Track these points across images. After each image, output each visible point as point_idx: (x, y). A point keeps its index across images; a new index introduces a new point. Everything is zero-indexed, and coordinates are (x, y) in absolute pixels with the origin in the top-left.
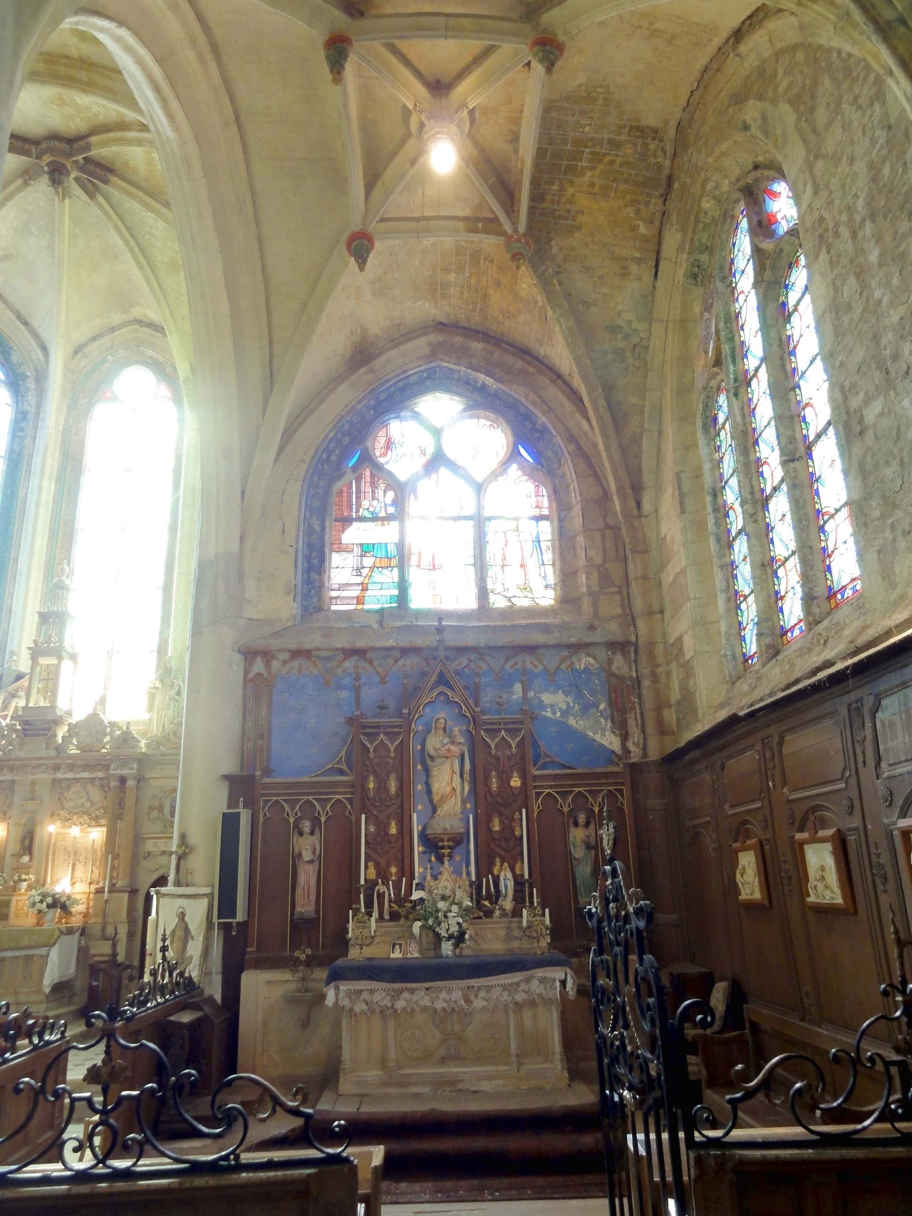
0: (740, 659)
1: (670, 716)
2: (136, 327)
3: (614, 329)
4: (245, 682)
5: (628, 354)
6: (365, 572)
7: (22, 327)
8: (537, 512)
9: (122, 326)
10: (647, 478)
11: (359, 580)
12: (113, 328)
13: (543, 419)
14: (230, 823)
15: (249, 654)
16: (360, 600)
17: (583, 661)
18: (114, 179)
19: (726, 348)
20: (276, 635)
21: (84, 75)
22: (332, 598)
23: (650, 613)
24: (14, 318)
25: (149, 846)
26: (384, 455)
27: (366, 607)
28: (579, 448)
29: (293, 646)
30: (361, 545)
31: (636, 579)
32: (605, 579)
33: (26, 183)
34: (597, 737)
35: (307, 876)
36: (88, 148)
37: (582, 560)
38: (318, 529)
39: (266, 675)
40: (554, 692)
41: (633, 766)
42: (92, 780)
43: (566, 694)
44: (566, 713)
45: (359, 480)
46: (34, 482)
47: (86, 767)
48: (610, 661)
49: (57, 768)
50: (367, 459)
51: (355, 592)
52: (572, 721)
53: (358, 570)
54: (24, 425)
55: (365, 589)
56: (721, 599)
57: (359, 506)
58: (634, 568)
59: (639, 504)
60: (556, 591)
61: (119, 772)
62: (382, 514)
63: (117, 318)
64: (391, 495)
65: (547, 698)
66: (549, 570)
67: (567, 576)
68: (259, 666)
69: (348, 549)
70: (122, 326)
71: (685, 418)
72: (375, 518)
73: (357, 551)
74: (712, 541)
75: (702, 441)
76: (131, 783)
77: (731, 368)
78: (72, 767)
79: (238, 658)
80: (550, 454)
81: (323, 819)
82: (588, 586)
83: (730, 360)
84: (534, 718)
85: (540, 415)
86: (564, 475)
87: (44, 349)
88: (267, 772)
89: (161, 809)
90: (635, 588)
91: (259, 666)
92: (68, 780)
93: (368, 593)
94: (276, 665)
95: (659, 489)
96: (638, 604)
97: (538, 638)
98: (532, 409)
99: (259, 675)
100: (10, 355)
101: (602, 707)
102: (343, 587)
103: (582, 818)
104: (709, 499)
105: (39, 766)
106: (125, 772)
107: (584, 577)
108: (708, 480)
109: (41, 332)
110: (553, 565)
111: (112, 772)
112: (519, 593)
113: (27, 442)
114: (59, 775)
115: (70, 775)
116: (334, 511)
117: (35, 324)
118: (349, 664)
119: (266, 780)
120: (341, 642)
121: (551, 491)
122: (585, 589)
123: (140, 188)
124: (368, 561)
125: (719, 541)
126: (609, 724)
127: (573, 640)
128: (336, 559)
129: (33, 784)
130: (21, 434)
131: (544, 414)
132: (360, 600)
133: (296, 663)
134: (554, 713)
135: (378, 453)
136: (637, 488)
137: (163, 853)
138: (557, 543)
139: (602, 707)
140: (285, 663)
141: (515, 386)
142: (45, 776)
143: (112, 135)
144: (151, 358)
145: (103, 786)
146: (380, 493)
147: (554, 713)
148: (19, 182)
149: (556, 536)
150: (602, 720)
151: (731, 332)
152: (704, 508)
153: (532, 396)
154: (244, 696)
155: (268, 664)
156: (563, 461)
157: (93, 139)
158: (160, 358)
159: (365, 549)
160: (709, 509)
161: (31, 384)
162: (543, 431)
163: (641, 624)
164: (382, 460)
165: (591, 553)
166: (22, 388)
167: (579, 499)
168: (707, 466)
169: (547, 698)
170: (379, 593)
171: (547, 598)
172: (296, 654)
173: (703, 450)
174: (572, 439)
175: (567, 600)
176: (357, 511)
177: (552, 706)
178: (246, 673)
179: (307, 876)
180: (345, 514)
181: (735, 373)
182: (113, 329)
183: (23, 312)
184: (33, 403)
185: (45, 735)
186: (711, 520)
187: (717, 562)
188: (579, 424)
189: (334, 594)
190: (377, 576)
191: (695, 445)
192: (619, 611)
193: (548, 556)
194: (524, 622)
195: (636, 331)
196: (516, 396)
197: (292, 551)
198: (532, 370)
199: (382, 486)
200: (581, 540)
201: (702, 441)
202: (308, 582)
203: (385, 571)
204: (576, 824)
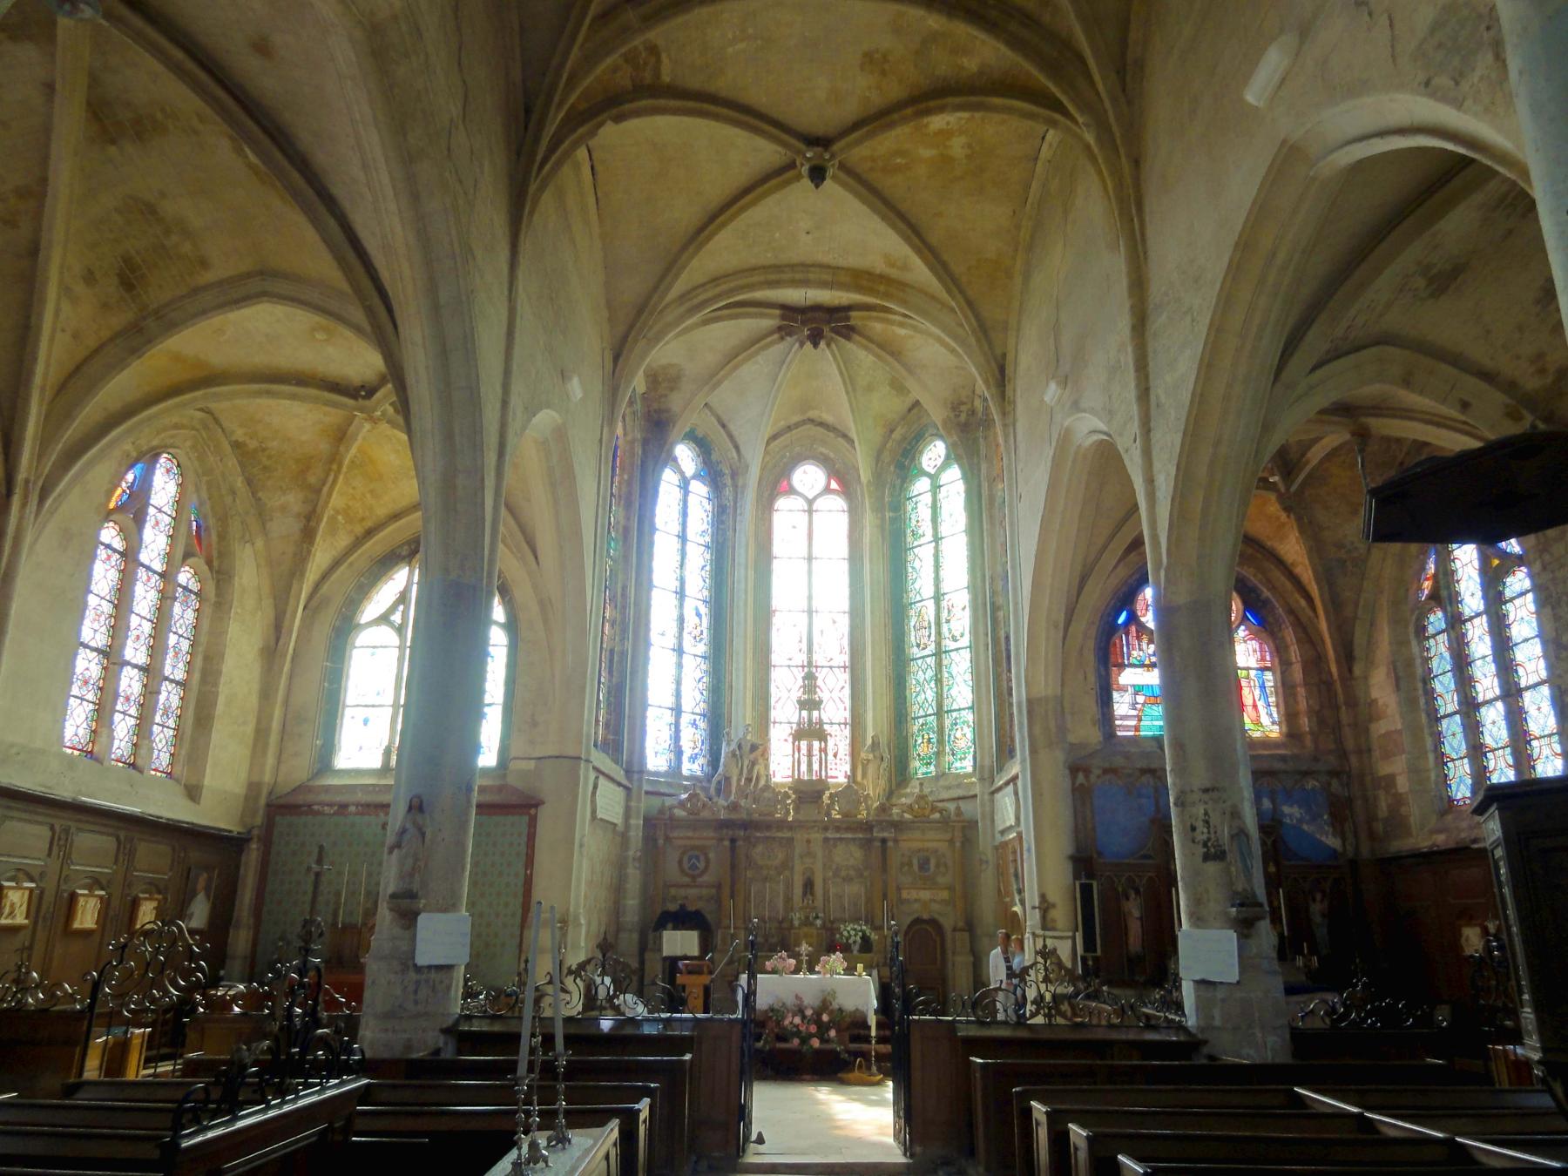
0: (1446, 800)
1: (1379, 827)
2: (808, 426)
3: (1339, 545)
4: (1074, 790)
5: (1348, 563)
6: (1139, 706)
7: (722, 431)
8: (1262, 665)
9: (797, 425)
10: (1358, 652)
11: (1134, 713)
12: (789, 427)
13: (1266, 593)
14: (1086, 891)
15: (1074, 770)
16: (1137, 728)
17: (1311, 784)
18: (856, 337)
19: (1444, 593)
20: (1091, 755)
21: (882, 288)
22: (1119, 726)
23: (1359, 752)
24: (716, 423)
25: (905, 895)
26: (1144, 616)
27: (1142, 733)
28: (1297, 618)
29: (1107, 765)
30: (1134, 686)
31: (1349, 725)
32: (1321, 722)
33: (782, 338)
34: (1323, 839)
35: (1135, 929)
36: (848, 319)
37: (1303, 705)
38: (1103, 673)
39: (1086, 783)
40: (1291, 806)
41: (1354, 863)
42: (854, 839)
43: (1300, 807)
44: (1300, 821)
45: (1127, 635)
46: (740, 573)
47: (848, 829)
48: (1329, 784)
49: (826, 829)
50: (1133, 618)
51: (1133, 723)
52: (1305, 827)
53: (1134, 705)
54: (724, 517)
55: (1140, 720)
56: (1431, 757)
57: (1129, 655)
58: (1344, 715)
59: (1350, 671)
60: (1281, 728)
61: (881, 835)
62: (1147, 662)
63: (796, 419)
64: (1152, 647)
65: (1286, 809)
66: (1274, 710)
67: (1290, 717)
68: (1081, 778)
69: (1123, 689)
70: (797, 425)
71: (1397, 622)
72: (1142, 665)
73: (1131, 690)
74: (1424, 716)
75: (1414, 643)
76: (890, 844)
77: (1449, 608)
78: (838, 829)
79: (1067, 772)
80: (1271, 619)
81: (1142, 890)
82: (1310, 728)
83: (1447, 602)
84: (1280, 823)
85: (1265, 590)
86: (1283, 638)
87: (737, 448)
88: (1100, 854)
89: (910, 864)
90: (1347, 732)
91: (1081, 778)
92: (834, 839)
93: (1142, 723)
94: (1093, 778)
95: (1370, 663)
96: (1350, 744)
97: (1279, 766)
98: (1260, 586)
99: (1081, 785)
100: (710, 454)
101: (1325, 817)
102: (1123, 718)
103: (1319, 896)
104: (1420, 685)
105: (815, 826)
106: (886, 835)
107: (1306, 720)
108: (1419, 671)
109: (735, 433)
110: (1277, 706)
111: (875, 834)
112: (1252, 727)
113: (730, 533)
114: (829, 835)
115: (838, 836)
116: (1112, 659)
117: (732, 427)
118: (1146, 779)
119: (1101, 861)
120: (1140, 764)
121: (1273, 649)
122: (1308, 729)
123: (870, 340)
124: (1140, 699)
125: (1428, 715)
126: (1331, 830)
127: (1304, 768)
128: (1116, 695)
129: (808, 841)
130: (722, 527)
131: (1269, 590)
132: (1137, 728)
133: (1107, 777)
134: (1292, 820)
135: (1139, 614)
136: (1347, 656)
137: (916, 900)
138: (1280, 690)
139: (1325, 817)
140: (1098, 777)
141: (1245, 567)
142: (817, 835)
143: (875, 314)
144: (822, 454)
145: (867, 844)
146: (1144, 646)
147: (1292, 820)
148: (776, 336)
149: (1279, 684)
150: (1326, 828)
151: (1448, 582)
152: (1415, 689)
153: (1260, 576)
154: (1074, 800)
155: (1087, 777)
156: (1283, 626)
157: (853, 314)
158: (832, 455)
159: (1138, 690)
160: (1421, 692)
161: (729, 481)
162: (1266, 602)
163: (1354, 760)
164: (1143, 619)
165: (1311, 702)
166: (720, 484)
167: (1299, 659)
168: (1418, 661)
169: (1286, 809)
170: (1149, 723)
171: (1274, 732)
172: (1106, 771)
173: (1415, 649)
174: (1291, 612)
175: (1292, 734)
176: (1128, 659)
177: (1291, 816)
178: (1073, 784)
179: (1135, 929)
180: (1120, 661)
181: (1452, 612)
182: (789, 428)
183: (725, 418)
184: (731, 498)
185: (817, 802)
186: (1422, 701)
187: (1426, 731)
188: (1297, 602)
189: (1117, 722)
190: (1147, 709)
191: (1408, 642)
192: (1332, 746)
193: (1272, 699)
194: (1266, 752)
195: (1356, 548)
196: (1247, 575)
197: (1093, 692)
198: (1259, 556)
199: (1145, 642)
200: (1301, 692)
201: (1414, 643)
202: (1103, 714)
203: (1154, 707)
204: (1314, 900)
